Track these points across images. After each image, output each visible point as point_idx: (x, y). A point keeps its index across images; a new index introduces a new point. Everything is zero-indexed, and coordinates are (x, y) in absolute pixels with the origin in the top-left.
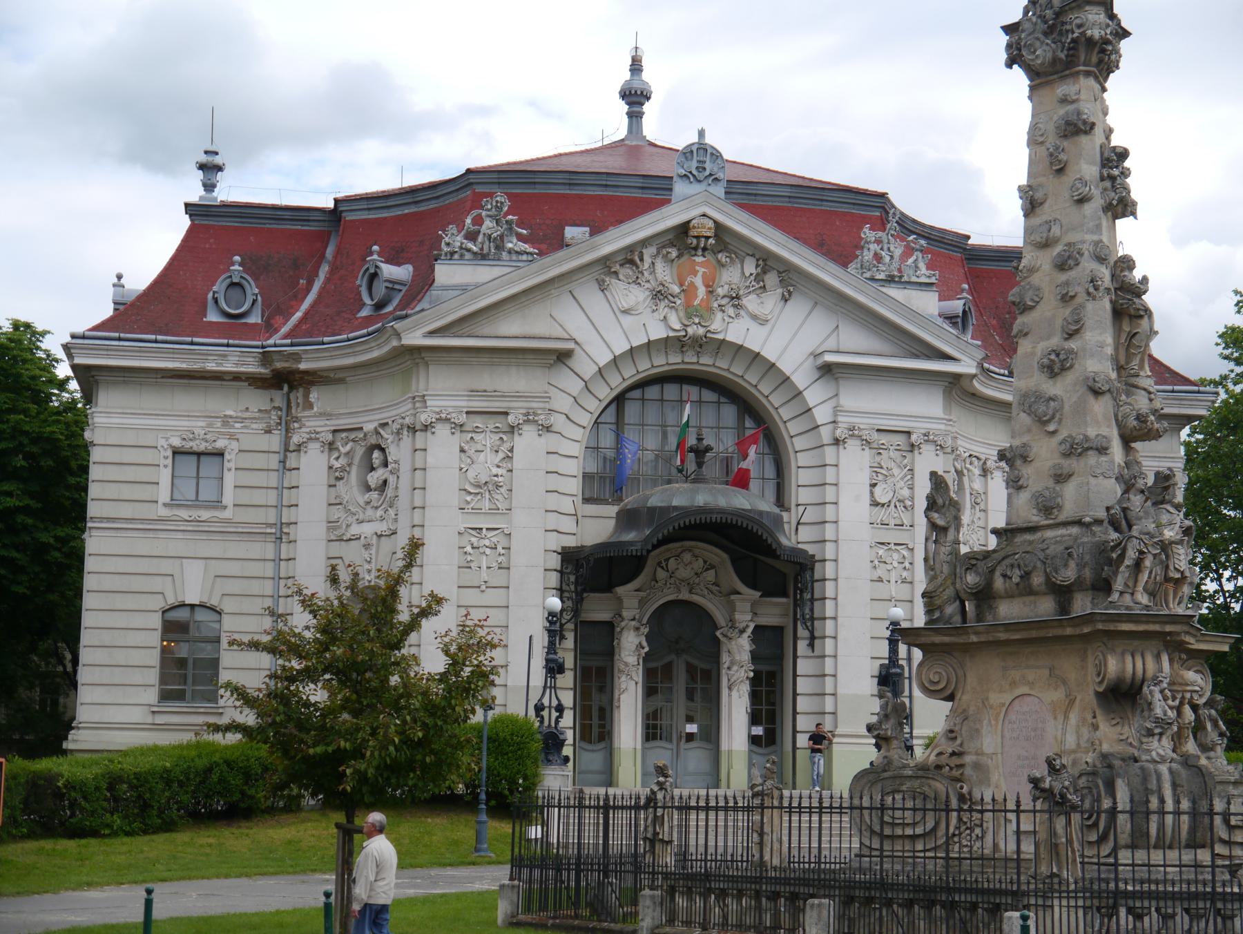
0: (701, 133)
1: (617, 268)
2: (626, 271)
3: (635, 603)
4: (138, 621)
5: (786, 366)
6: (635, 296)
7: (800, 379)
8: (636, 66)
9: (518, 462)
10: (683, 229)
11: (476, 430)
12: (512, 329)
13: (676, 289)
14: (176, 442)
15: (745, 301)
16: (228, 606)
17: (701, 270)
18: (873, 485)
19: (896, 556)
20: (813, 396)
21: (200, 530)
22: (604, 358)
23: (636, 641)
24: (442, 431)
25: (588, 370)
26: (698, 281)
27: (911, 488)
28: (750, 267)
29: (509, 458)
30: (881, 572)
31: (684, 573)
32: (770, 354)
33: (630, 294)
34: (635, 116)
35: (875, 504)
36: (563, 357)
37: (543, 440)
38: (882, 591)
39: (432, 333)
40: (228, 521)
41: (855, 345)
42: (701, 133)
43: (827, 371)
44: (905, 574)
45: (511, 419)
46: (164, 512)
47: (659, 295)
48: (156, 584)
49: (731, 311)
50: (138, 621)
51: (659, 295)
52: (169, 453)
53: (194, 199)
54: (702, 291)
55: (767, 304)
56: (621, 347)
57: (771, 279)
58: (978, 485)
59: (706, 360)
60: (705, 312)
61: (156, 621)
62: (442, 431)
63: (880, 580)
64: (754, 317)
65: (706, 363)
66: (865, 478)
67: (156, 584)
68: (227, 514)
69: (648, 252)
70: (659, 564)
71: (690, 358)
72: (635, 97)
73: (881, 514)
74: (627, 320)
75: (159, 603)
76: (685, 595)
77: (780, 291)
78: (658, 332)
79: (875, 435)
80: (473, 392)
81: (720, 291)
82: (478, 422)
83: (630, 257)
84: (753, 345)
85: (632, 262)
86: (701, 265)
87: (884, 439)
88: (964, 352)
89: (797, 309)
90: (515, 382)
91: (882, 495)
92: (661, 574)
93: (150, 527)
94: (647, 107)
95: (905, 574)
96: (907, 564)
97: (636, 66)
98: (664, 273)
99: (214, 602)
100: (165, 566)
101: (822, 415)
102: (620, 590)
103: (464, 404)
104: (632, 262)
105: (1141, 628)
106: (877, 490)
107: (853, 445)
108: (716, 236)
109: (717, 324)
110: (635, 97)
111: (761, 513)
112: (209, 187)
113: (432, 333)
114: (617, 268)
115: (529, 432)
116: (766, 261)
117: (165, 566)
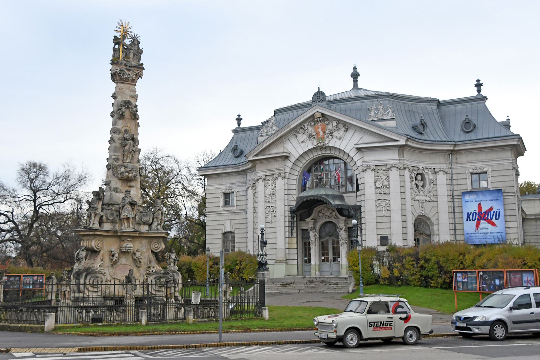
0: (319, 88)
1: (298, 130)
2: (301, 131)
3: (312, 223)
4: (217, 237)
5: (347, 151)
6: (305, 137)
7: (351, 154)
8: (355, 68)
9: (277, 188)
10: (313, 115)
11: (268, 180)
12: (276, 151)
13: (314, 134)
14: (223, 191)
15: (334, 134)
16: (236, 231)
17: (320, 127)
18: (376, 182)
19: (384, 203)
20: (355, 159)
21: (229, 213)
22: (297, 156)
23: (314, 234)
24: (261, 181)
25: (293, 160)
26: (320, 130)
27: (389, 182)
28: (334, 124)
29: (275, 187)
30: (379, 209)
31: (328, 214)
32: (342, 148)
33: (302, 137)
34: (355, 81)
35: (376, 188)
36: (287, 157)
37: (283, 181)
38: (380, 214)
39: (256, 156)
40: (235, 210)
41: (367, 140)
42: (319, 88)
43: (359, 149)
44: (388, 208)
45: (274, 176)
46: (222, 209)
47: (310, 136)
48: (221, 227)
49: (330, 137)
50: (217, 237)
51: (310, 136)
52: (222, 194)
53: (234, 128)
54: (321, 133)
55: (341, 132)
56: (301, 152)
57: (341, 126)
58: (431, 177)
59: (328, 152)
60: (322, 139)
61: (221, 236)
62: (261, 181)
63: (380, 211)
64: (337, 138)
65: (328, 153)
66: (373, 180)
67: (221, 227)
68: (235, 208)
69: (306, 125)
70: (319, 212)
71: (324, 152)
72: (355, 76)
73: (379, 191)
74: (302, 145)
75: (221, 232)
76: (328, 220)
77: (344, 129)
78: (311, 147)
79: (375, 167)
80: (267, 170)
81: (327, 132)
82: (268, 178)
83: (301, 126)
84: (337, 146)
85: (302, 128)
86: (320, 125)
87: (379, 168)
88: (400, 138)
89: (350, 133)
90: (276, 165)
91: (378, 185)
92: (320, 214)
93: (219, 213)
94: (359, 79)
95: (388, 208)
96: (388, 205)
97: (355, 68)
98: (311, 130)
99: (233, 231)
100: (222, 222)
101: (359, 163)
102: (306, 220)
103: (264, 173)
104: (302, 128)
105: (85, 233)
106: (377, 184)
107: (369, 171)
108: (323, 117)
109: (326, 142)
110: (355, 76)
111: (328, 196)
112: (239, 124)
113: (256, 156)
114: (298, 130)
115: (280, 178)
116: (339, 121)
117: (222, 222)
